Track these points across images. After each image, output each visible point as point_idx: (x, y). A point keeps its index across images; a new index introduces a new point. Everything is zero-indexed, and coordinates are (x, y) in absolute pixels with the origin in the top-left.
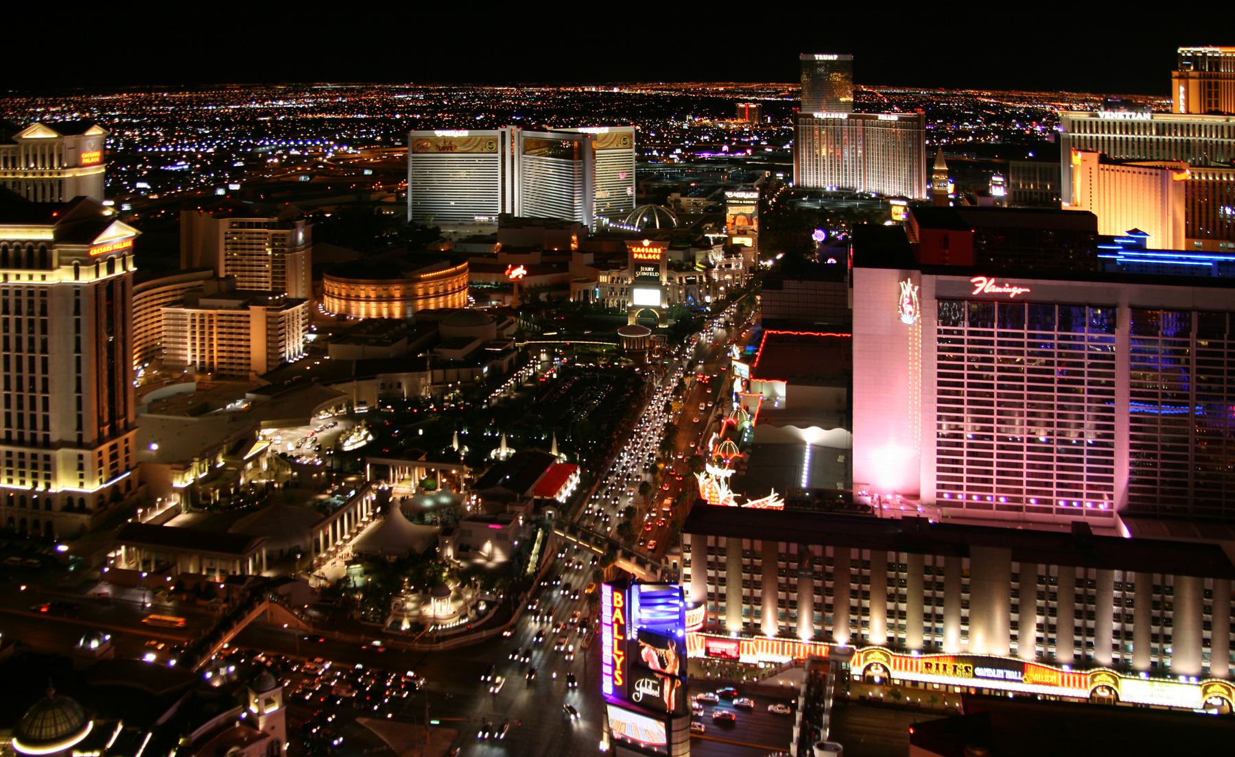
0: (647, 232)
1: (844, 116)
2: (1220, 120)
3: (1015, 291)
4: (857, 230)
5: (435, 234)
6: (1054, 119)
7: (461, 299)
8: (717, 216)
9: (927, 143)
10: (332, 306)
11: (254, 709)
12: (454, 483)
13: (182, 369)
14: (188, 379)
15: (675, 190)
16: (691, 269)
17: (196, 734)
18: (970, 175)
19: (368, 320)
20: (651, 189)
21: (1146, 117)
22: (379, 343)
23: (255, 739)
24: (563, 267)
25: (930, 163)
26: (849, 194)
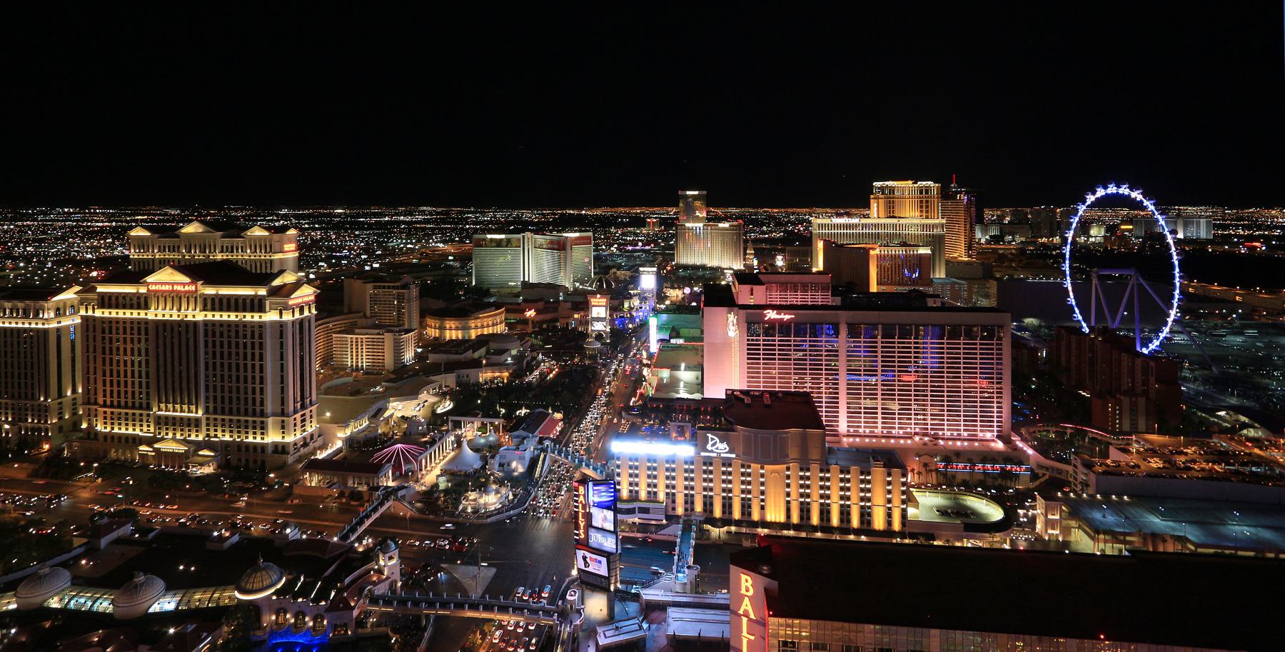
0: (600, 291)
1: (701, 225)
2: (894, 221)
3: (787, 317)
4: (706, 286)
5: (487, 293)
6: (810, 222)
7: (501, 329)
8: (634, 280)
9: (740, 242)
10: (432, 333)
11: (382, 563)
12: (496, 429)
13: (344, 368)
14: (348, 375)
15: (613, 267)
16: (621, 310)
17: (347, 580)
18: (765, 254)
19: (451, 341)
20: (603, 266)
21: (855, 221)
22: (457, 353)
23: (381, 581)
24: (555, 310)
25: (745, 250)
26: (704, 267)
